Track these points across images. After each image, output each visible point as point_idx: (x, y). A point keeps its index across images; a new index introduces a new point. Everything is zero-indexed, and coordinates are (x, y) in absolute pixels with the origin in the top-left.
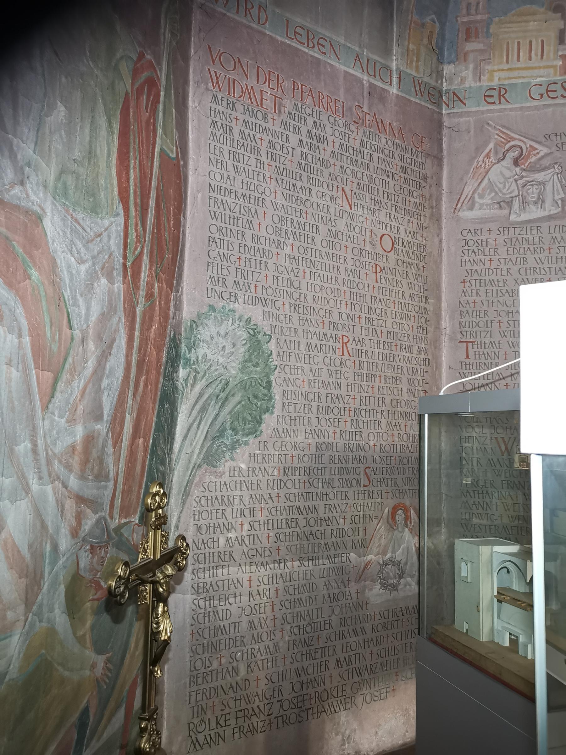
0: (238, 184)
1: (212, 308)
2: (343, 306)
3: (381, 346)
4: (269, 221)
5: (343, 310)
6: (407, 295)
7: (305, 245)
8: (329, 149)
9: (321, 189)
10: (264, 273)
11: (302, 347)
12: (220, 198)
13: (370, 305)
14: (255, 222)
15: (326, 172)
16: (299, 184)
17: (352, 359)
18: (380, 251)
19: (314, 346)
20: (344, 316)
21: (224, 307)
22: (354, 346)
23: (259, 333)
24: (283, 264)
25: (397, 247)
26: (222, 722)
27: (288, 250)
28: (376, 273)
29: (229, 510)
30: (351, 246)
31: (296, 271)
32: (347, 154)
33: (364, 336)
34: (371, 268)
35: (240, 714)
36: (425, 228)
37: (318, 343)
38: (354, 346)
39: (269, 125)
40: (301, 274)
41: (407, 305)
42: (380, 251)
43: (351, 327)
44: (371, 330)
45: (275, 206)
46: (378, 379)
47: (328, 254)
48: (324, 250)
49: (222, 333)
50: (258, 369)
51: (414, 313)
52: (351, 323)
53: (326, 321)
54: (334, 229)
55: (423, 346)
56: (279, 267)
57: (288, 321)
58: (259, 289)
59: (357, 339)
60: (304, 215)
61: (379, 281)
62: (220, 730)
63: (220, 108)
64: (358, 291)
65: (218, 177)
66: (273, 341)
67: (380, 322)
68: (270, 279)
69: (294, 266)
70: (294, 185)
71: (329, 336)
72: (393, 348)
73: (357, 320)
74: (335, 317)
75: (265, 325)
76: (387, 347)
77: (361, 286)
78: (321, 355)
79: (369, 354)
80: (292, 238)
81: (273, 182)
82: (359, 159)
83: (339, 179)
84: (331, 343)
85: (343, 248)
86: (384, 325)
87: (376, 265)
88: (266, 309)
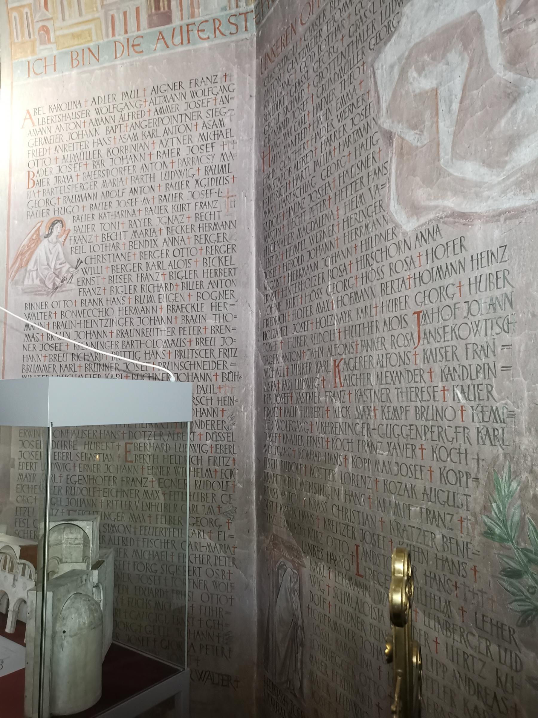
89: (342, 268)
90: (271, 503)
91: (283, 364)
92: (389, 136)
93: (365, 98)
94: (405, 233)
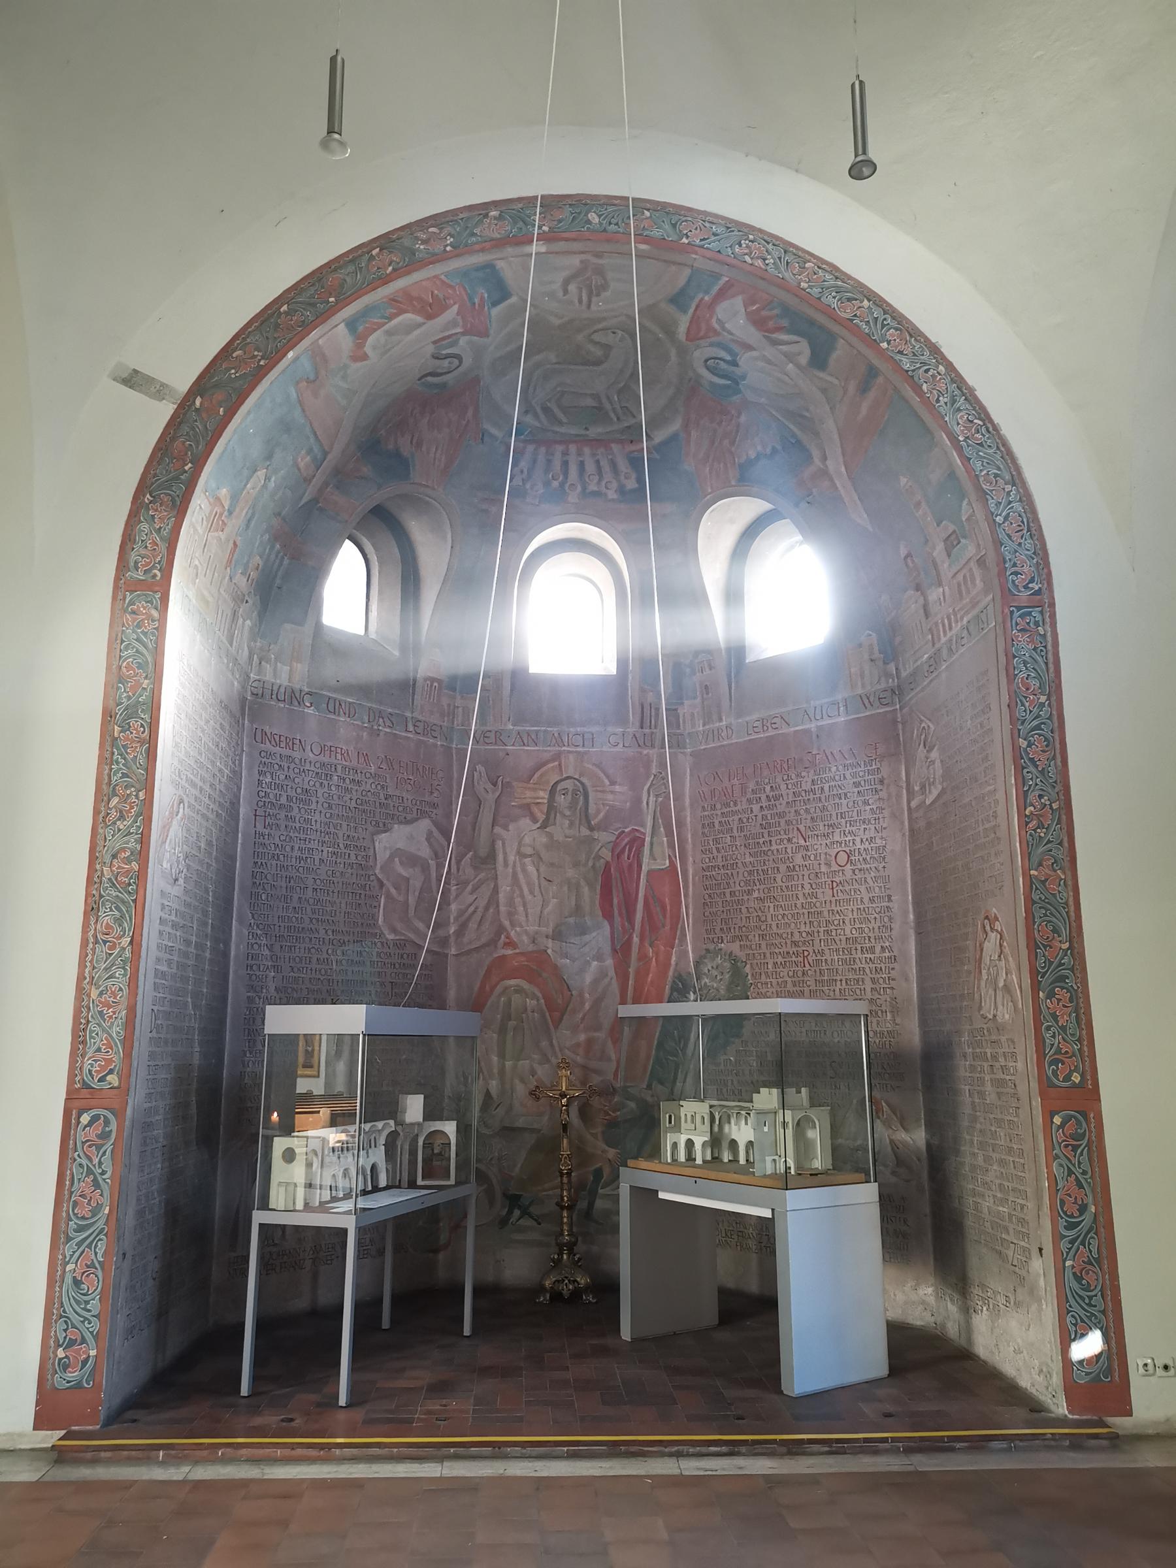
0: (720, 859)
1: (708, 951)
2: (803, 926)
3: (841, 953)
4: (741, 877)
5: (803, 929)
6: (866, 900)
7: (768, 886)
8: (784, 803)
9: (779, 837)
10: (739, 918)
11: (770, 966)
12: (708, 874)
13: (828, 919)
14: (731, 882)
15: (783, 822)
16: (761, 841)
17: (813, 969)
18: (836, 868)
19: (779, 963)
20: (804, 935)
21: (715, 948)
22: (814, 957)
23: (738, 961)
24: (753, 905)
25: (853, 858)
26: (729, 1234)
27: (756, 895)
28: (833, 888)
29: (725, 1090)
30: (806, 873)
31: (762, 908)
32: (801, 798)
33: (823, 947)
34: (827, 886)
35: (740, 1234)
36: (885, 828)
37: (783, 960)
38: (814, 957)
39: (739, 807)
40: (766, 910)
41: (866, 909)
42: (835, 867)
43: (811, 942)
44: (829, 941)
45: (745, 865)
46: (839, 983)
47: (787, 887)
48: (784, 885)
49: (715, 967)
50: (739, 988)
51: (876, 915)
52: (810, 938)
53: (789, 942)
54: (791, 865)
55: (887, 944)
56: (750, 910)
57: (758, 948)
58: (737, 930)
59: (817, 951)
60: (767, 863)
61: (835, 895)
62: (729, 1240)
63: (706, 813)
64: (816, 909)
65: (707, 860)
66: (748, 966)
67: (839, 931)
68: (744, 919)
69: (761, 905)
70: (758, 843)
71: (791, 952)
72: (854, 952)
73: (816, 934)
74: (797, 937)
75: (741, 955)
76: (846, 952)
77: (818, 904)
78: (786, 970)
79: (829, 962)
80: (758, 884)
81: (742, 847)
82: (812, 796)
83: (794, 822)
84: (794, 959)
85: (801, 877)
86: (842, 933)
87: (832, 882)
88: (742, 943)
89: (342, 941)
90: (250, 1109)
91: (275, 994)
92: (381, 885)
93: (367, 849)
94: (387, 940)
